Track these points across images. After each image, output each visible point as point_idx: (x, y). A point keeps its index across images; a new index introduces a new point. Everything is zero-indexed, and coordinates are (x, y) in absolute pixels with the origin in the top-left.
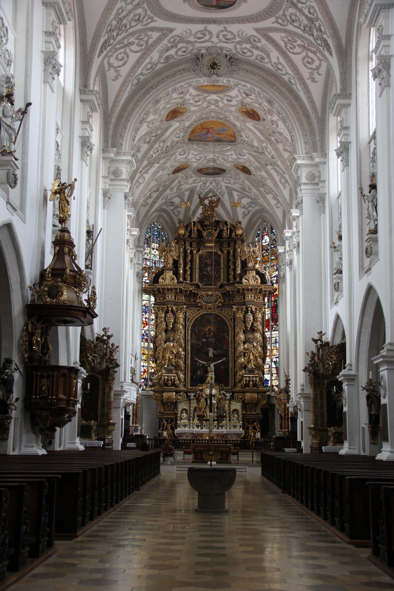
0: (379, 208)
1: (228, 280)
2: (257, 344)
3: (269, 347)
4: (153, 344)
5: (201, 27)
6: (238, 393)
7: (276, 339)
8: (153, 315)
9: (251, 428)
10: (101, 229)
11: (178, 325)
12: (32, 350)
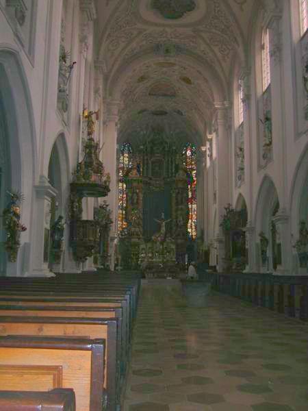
0: (273, 131)
1: (168, 175)
5: (161, 29)
10: (104, 143)
12: (73, 211)
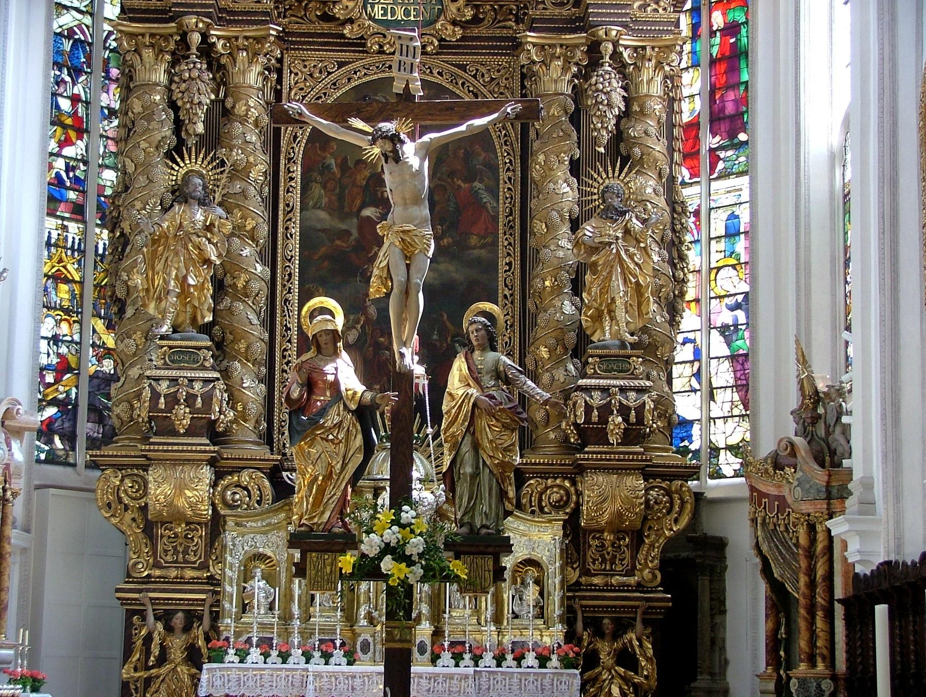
2: (644, 221)
3: (694, 258)
4: (112, 231)
6: (544, 475)
7: (733, 216)
8: (113, 86)
9: (605, 658)
11: (238, 128)
